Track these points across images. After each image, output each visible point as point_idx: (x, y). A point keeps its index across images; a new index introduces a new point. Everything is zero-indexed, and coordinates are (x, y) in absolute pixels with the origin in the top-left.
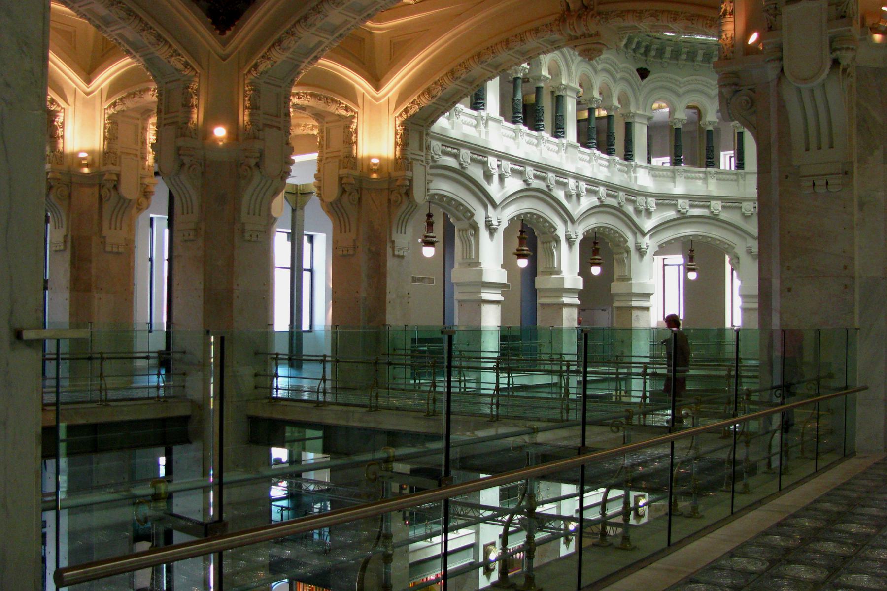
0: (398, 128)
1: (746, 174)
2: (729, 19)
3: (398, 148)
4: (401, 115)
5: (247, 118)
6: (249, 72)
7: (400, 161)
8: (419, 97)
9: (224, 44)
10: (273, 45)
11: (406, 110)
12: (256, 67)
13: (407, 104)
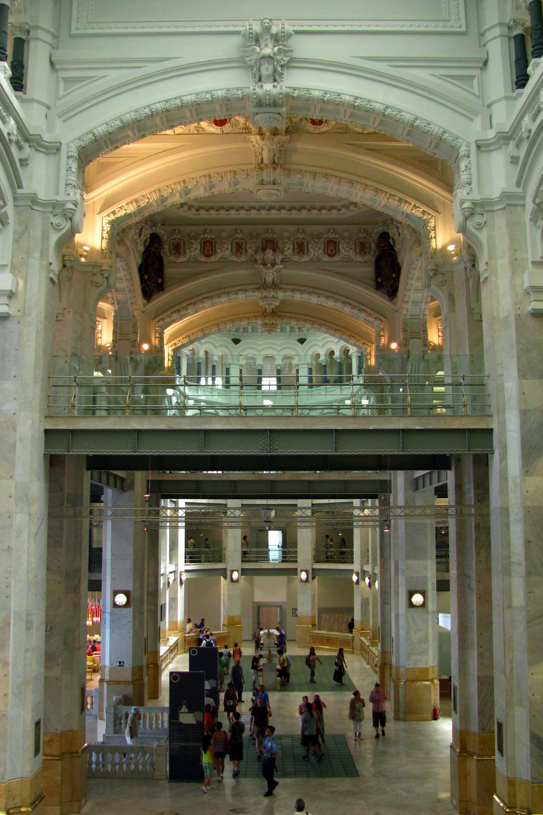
0: (170, 352)
1: (231, 391)
2: (383, 338)
3: (170, 362)
4: (172, 346)
5: (157, 342)
6: (159, 321)
7: (171, 368)
8: (183, 339)
9: (145, 305)
10: (175, 312)
11: (175, 344)
12: (163, 319)
13: (176, 341)
